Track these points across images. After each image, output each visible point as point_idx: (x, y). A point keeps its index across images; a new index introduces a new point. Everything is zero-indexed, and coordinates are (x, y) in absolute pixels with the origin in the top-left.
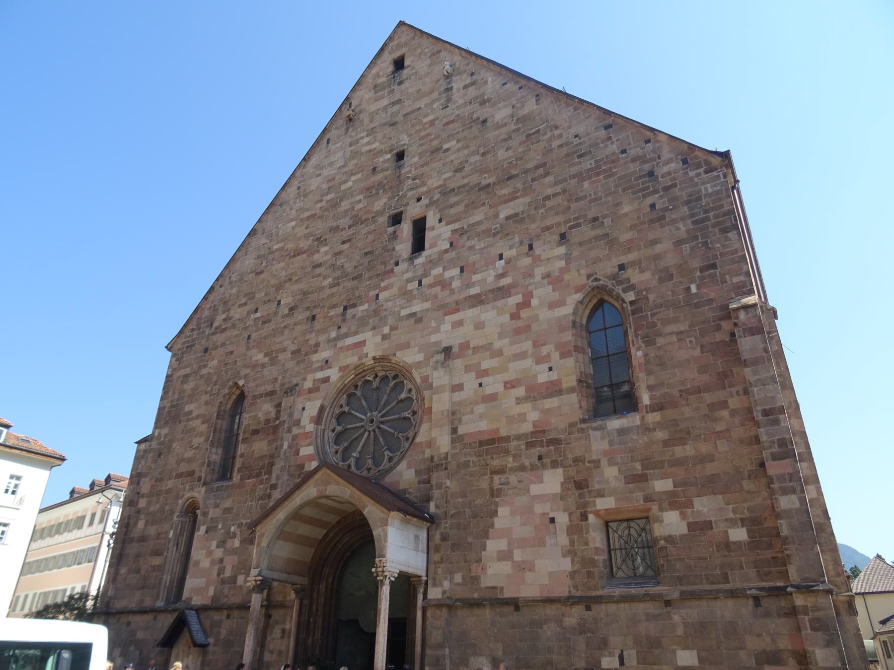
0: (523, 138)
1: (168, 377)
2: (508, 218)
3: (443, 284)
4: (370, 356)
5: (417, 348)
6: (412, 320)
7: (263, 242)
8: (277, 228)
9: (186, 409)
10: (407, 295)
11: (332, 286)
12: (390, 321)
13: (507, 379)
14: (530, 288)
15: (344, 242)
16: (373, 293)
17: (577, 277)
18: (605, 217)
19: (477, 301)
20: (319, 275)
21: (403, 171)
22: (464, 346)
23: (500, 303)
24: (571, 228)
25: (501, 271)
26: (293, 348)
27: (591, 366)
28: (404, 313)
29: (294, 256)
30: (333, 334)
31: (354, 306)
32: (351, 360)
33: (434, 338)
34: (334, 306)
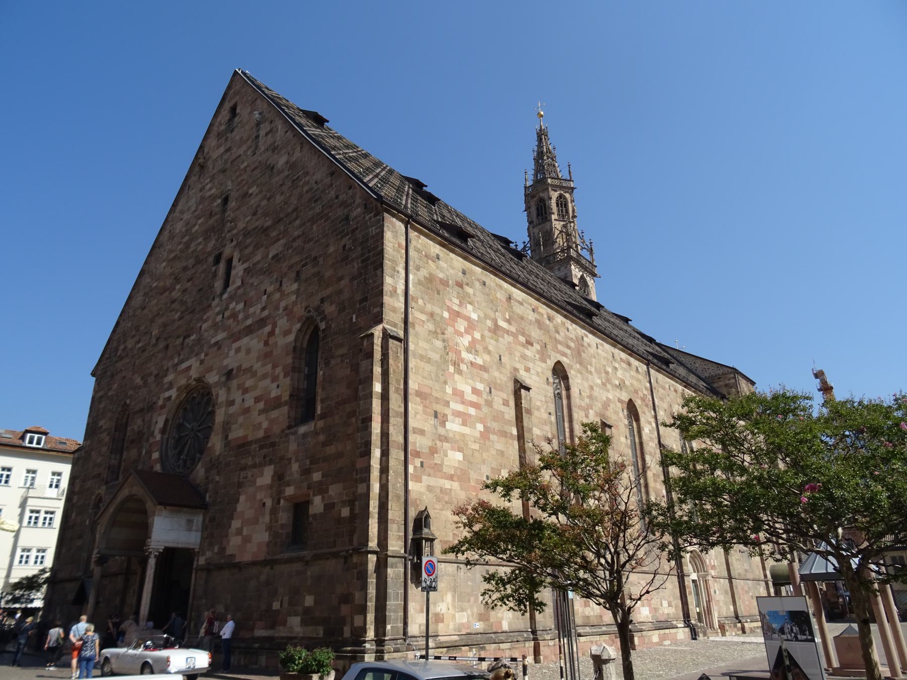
0: (290, 184)
1: (93, 398)
2: (273, 258)
3: (234, 316)
4: (193, 378)
5: (215, 372)
6: (216, 348)
7: (148, 281)
8: (156, 268)
9: (100, 425)
10: (215, 326)
11: (181, 318)
12: (205, 349)
13: (256, 395)
14: (277, 318)
15: (188, 281)
16: (199, 325)
17: (299, 311)
18: (320, 256)
19: (249, 331)
20: (173, 310)
21: (227, 214)
22: (239, 368)
23: (260, 332)
24: (303, 266)
25: (264, 305)
26: (155, 373)
27: (306, 382)
28: (213, 342)
29: (162, 294)
30: (176, 361)
31: (189, 336)
32: (183, 382)
33: (226, 362)
34: (178, 337)
